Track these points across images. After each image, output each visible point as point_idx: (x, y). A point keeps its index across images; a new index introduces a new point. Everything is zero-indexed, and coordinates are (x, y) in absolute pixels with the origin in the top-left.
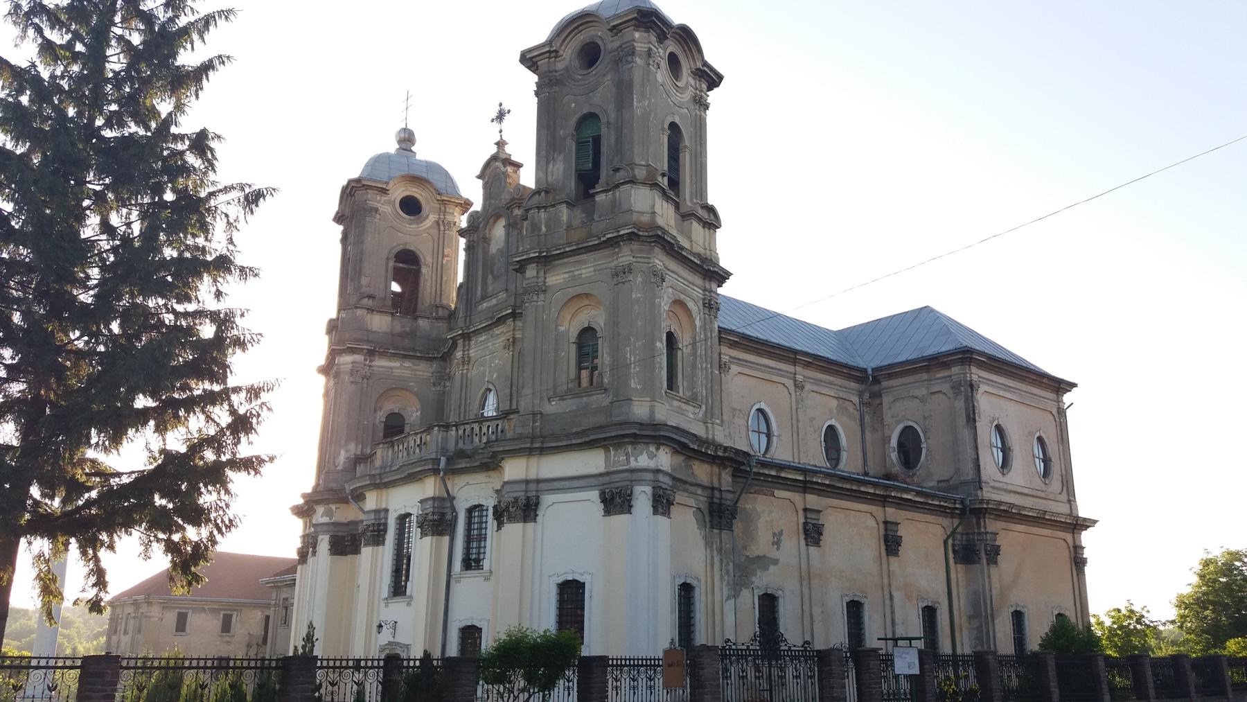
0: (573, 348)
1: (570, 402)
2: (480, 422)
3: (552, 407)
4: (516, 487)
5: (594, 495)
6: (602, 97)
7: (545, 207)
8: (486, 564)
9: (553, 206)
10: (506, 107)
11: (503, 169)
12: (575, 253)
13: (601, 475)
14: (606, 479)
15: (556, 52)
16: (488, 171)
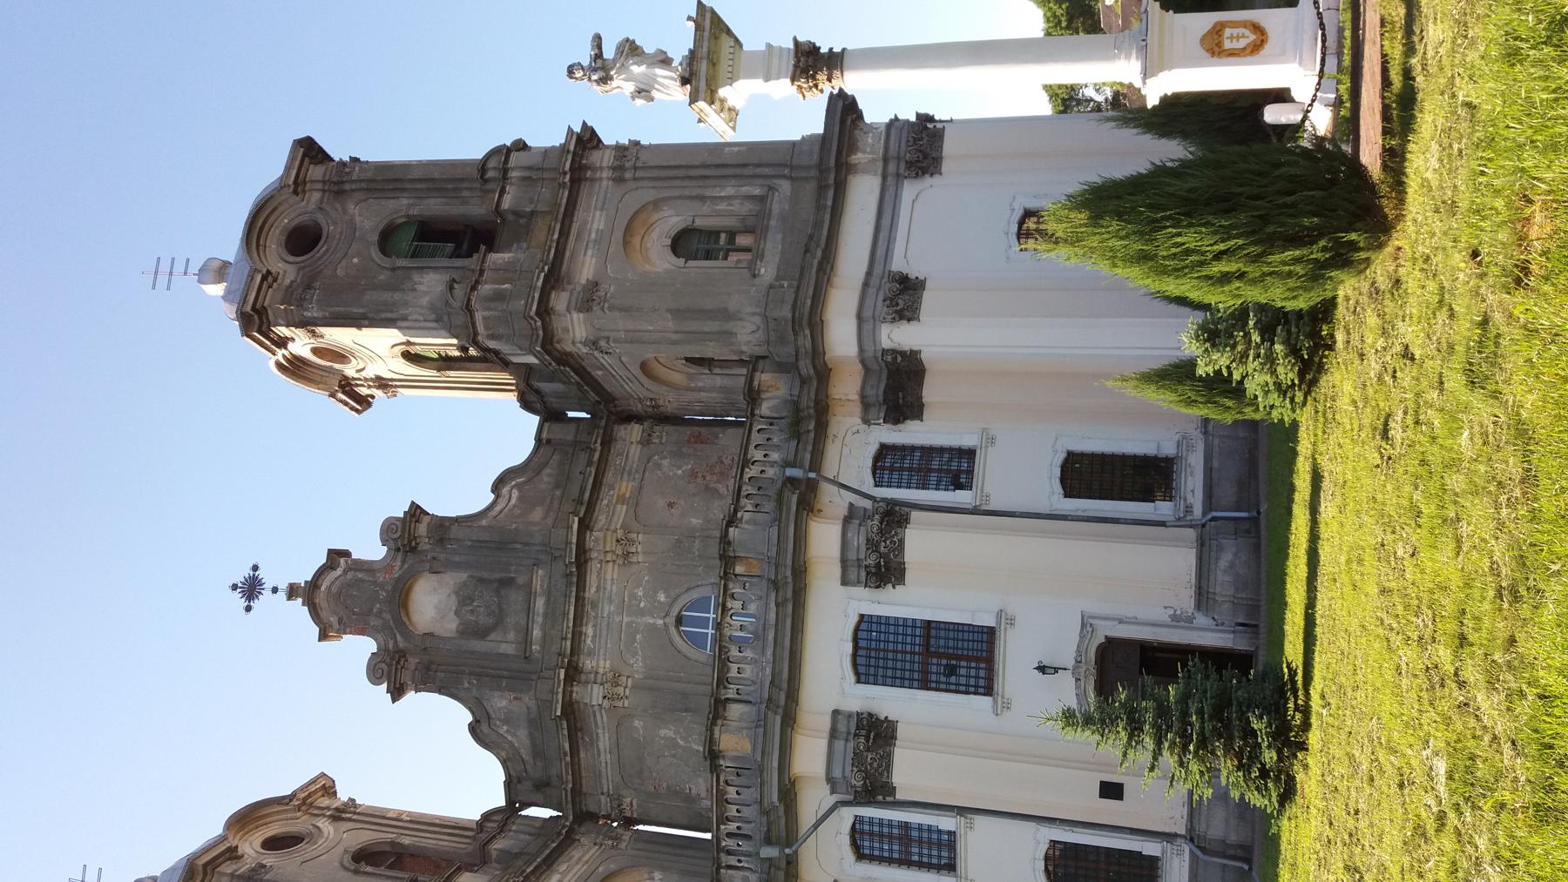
0: (691, 263)
1: (769, 246)
2: (746, 462)
3: (767, 272)
4: (869, 302)
5: (909, 189)
6: (368, 217)
7: (477, 282)
8: (967, 441)
9: (482, 272)
10: (241, 574)
11: (339, 571)
12: (564, 234)
13: (884, 178)
14: (892, 167)
15: (269, 272)
16: (323, 614)
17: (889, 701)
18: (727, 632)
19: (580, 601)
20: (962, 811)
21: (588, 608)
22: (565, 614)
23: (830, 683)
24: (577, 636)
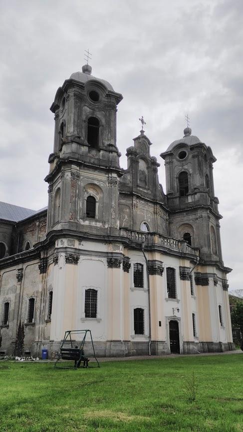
17: (165, 273)
18: (171, 240)
19: (148, 201)
20: (149, 290)
21: (147, 203)
22: (148, 198)
23: (168, 262)
24: (143, 199)
